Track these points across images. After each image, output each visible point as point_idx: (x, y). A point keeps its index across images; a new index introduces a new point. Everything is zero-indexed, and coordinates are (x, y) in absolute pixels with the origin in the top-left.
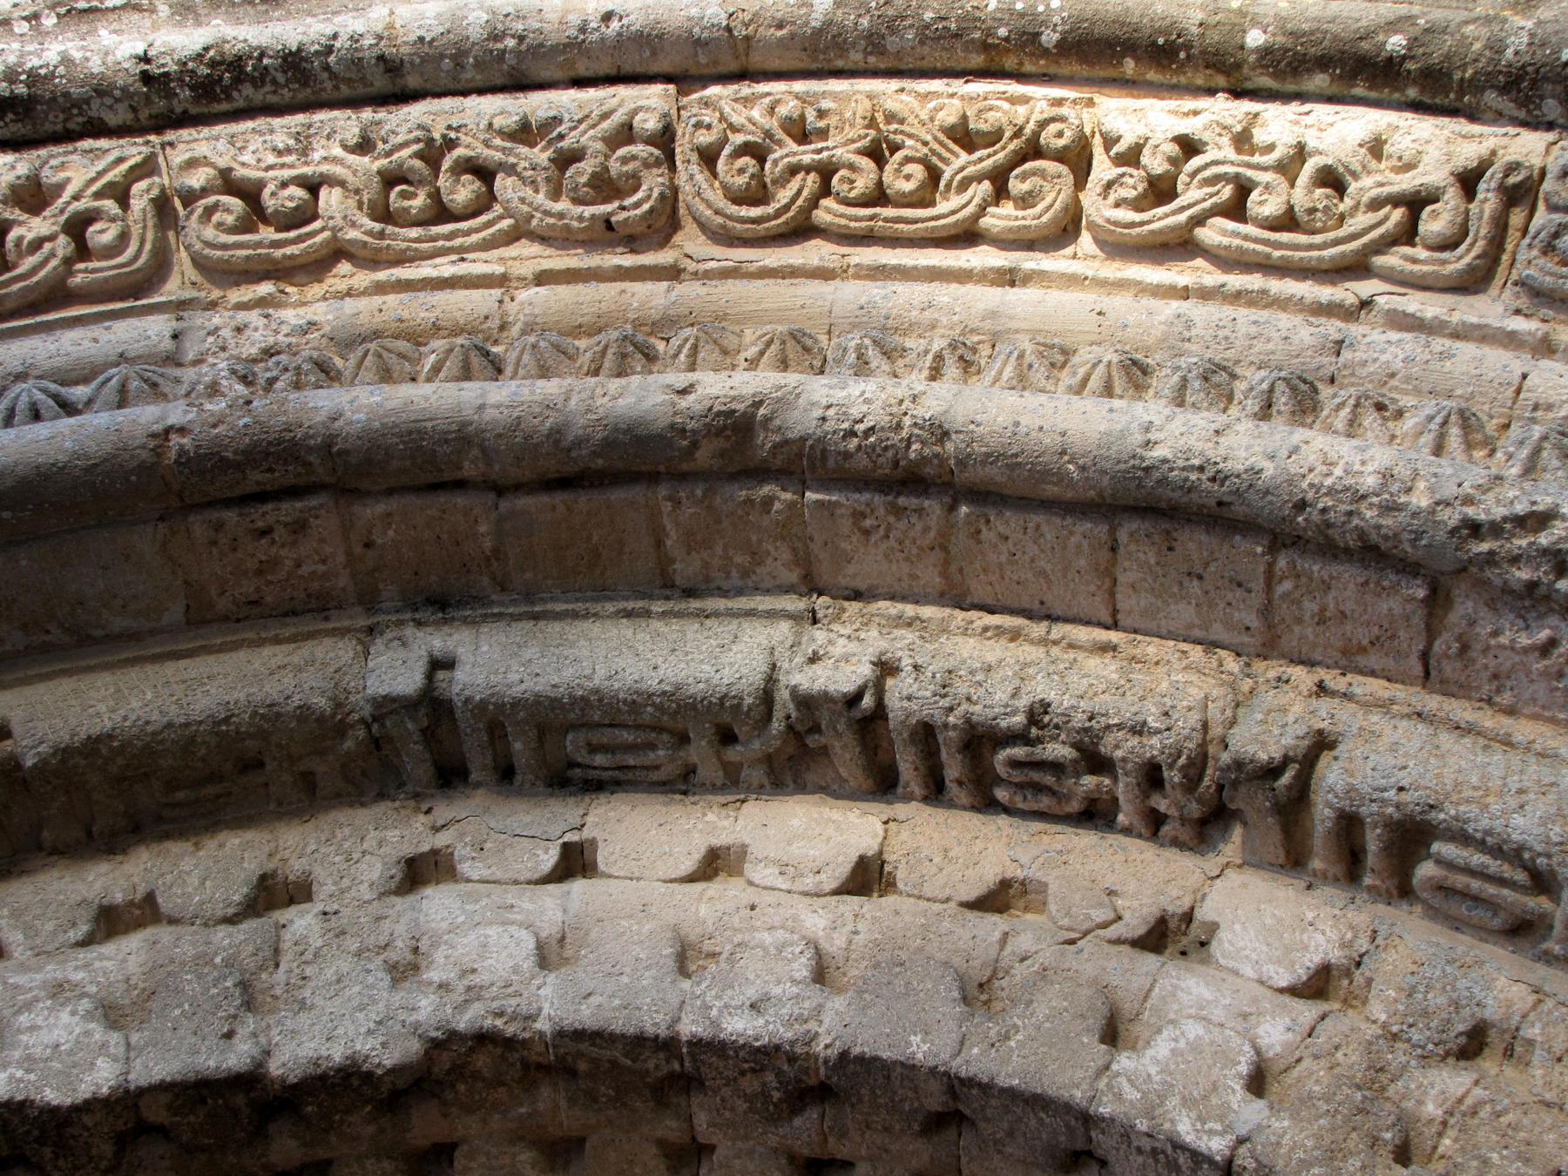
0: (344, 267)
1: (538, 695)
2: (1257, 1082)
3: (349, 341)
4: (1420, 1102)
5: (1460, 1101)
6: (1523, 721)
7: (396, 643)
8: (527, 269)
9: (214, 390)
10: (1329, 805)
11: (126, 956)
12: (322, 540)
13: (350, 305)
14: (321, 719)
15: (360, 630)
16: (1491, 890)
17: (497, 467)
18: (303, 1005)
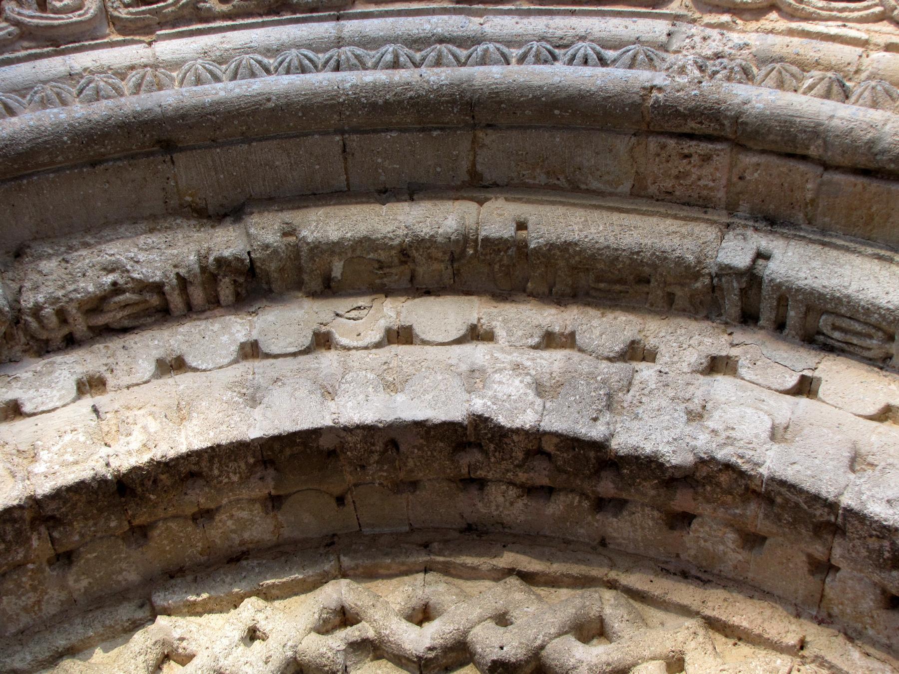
0: (774, 15)
1: (813, 289)
3: (764, 60)
7: (740, 237)
8: (882, 40)
9: (682, 70)
11: (554, 360)
12: (717, 169)
13: (771, 38)
14: (688, 267)
15: (721, 224)
17: (829, 154)
18: (637, 417)
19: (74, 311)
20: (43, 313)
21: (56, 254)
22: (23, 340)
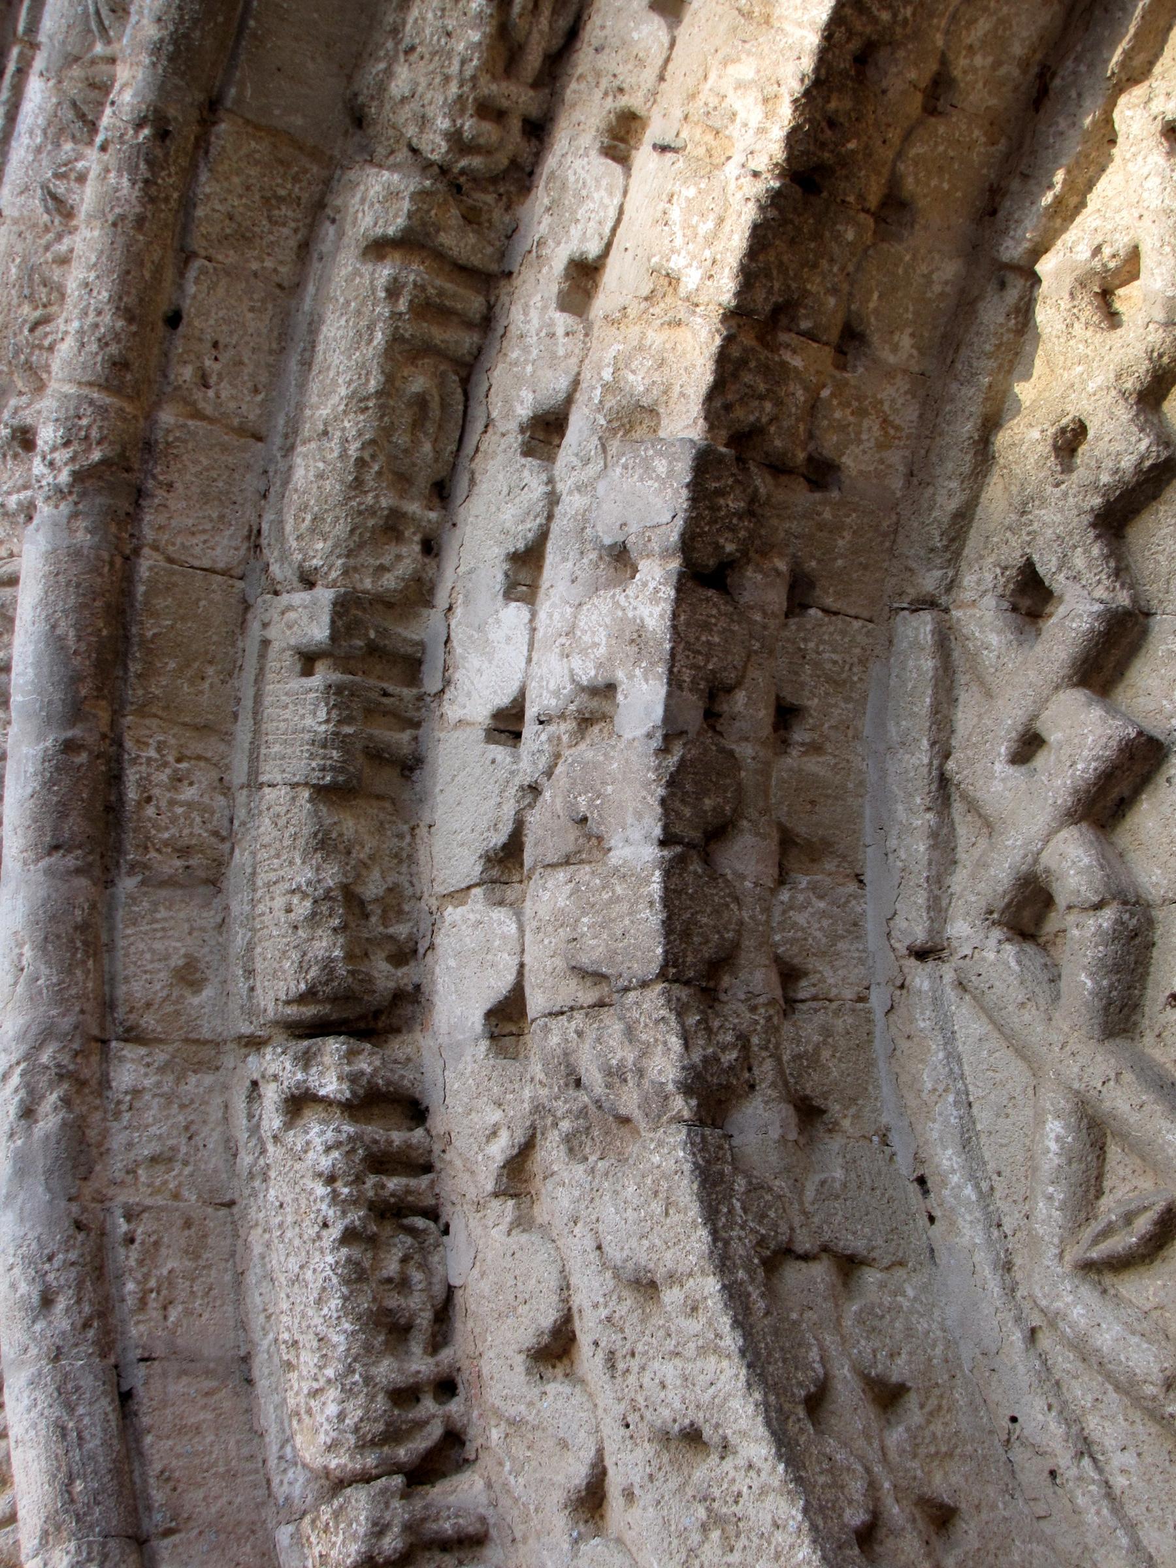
19: (494, 87)
20: (467, 135)
21: (392, 60)
22: (490, 198)
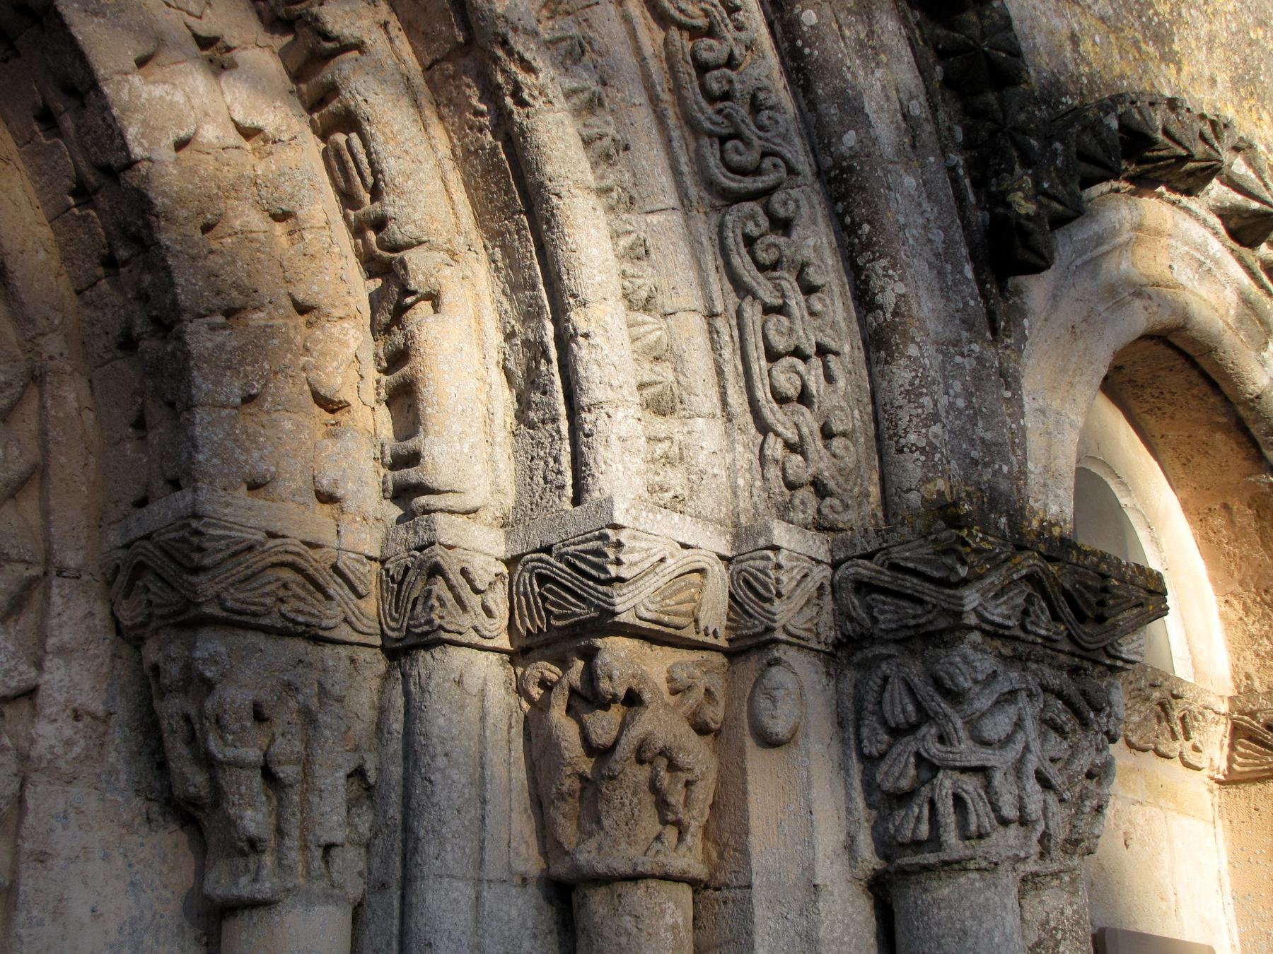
2: (181, 145)
4: (236, 217)
5: (251, 232)
6: (441, 126)
10: (329, 77)
16: (354, 172)
